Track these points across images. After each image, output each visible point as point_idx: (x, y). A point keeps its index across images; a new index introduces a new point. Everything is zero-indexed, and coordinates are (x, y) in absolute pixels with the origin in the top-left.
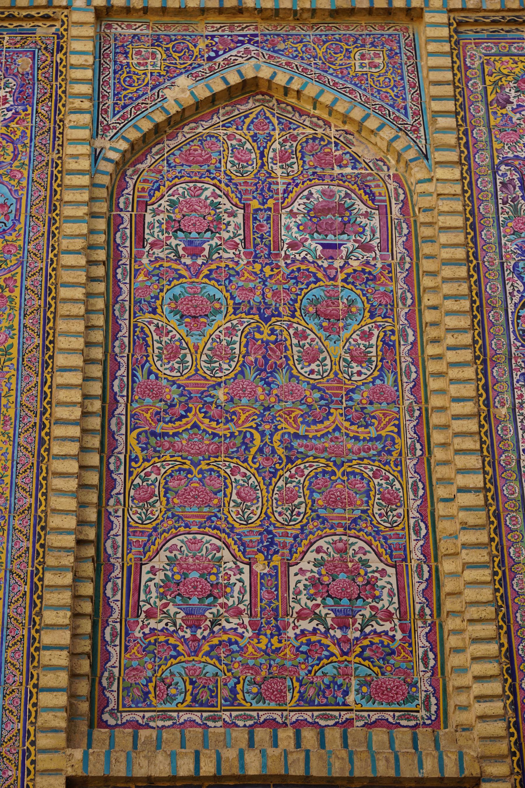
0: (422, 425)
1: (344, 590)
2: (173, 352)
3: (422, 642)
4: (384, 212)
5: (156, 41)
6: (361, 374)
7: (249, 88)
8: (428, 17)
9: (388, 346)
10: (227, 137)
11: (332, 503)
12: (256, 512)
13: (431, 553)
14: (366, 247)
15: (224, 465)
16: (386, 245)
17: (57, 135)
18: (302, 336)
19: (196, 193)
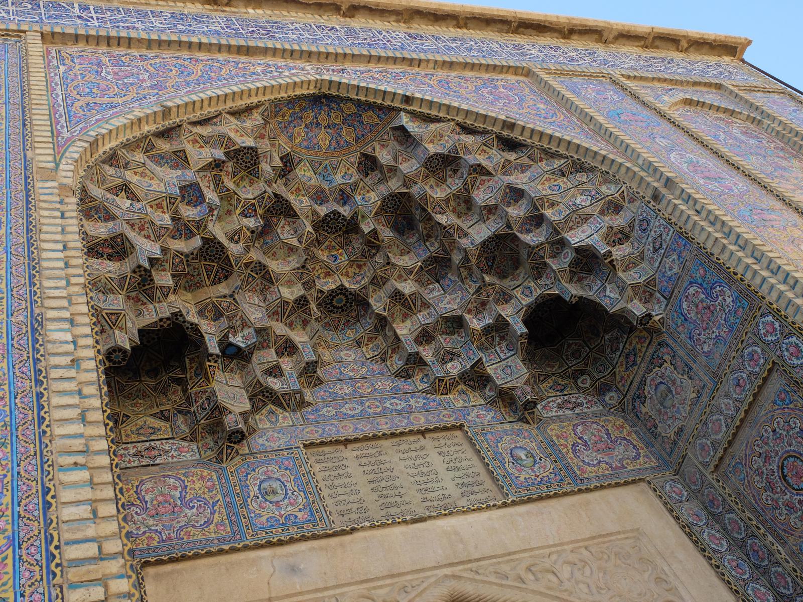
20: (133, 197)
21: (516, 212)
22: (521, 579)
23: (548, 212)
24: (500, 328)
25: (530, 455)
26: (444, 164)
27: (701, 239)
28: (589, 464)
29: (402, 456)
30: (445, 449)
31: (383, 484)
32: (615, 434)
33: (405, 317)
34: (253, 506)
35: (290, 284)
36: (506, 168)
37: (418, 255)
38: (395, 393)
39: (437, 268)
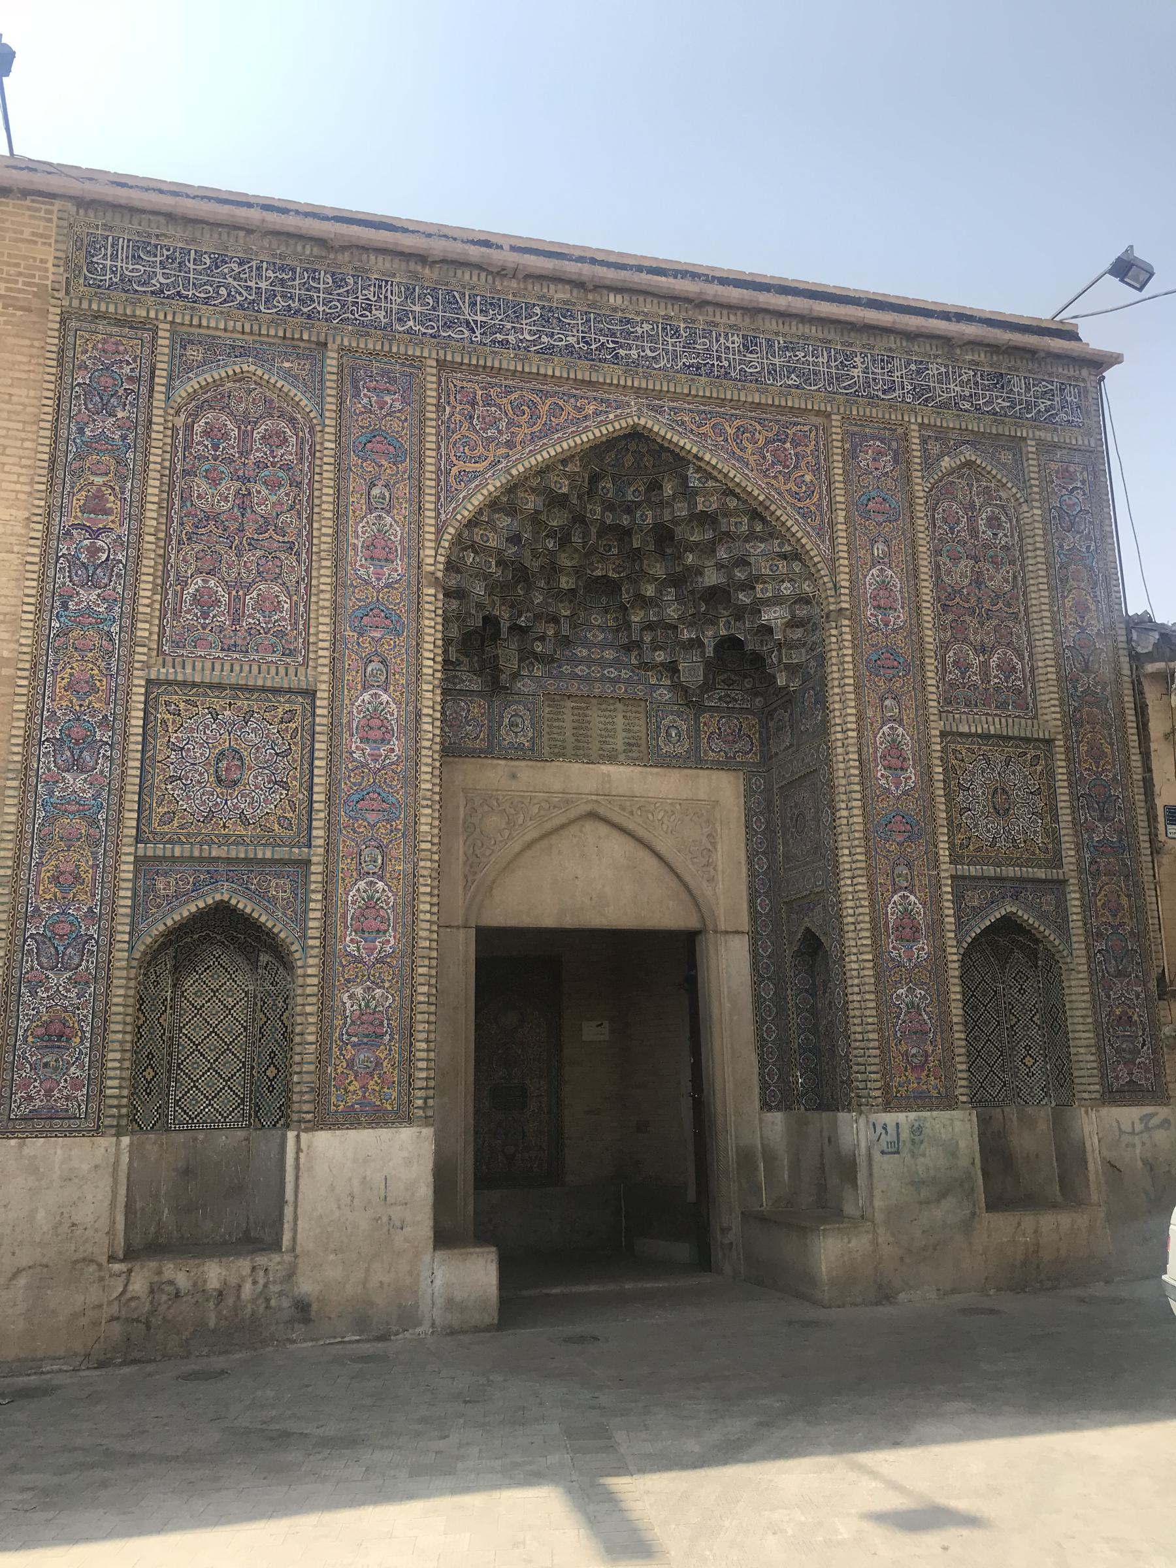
1: (1008, 670)
2: (949, 573)
3: (1029, 689)
5: (936, 439)
6: (1007, 587)
7: (969, 464)
9: (1015, 577)
11: (1002, 636)
12: (979, 638)
13: (1031, 656)
14: (1006, 536)
16: (1012, 536)
17: (909, 479)
18: (988, 570)
20: (476, 552)
21: (740, 575)
22: (632, 813)
23: (759, 587)
24: (697, 643)
25: (679, 734)
26: (706, 519)
27: (829, 670)
28: (713, 751)
29: (600, 713)
30: (629, 714)
31: (582, 732)
32: (745, 731)
33: (642, 608)
34: (503, 732)
35: (568, 575)
36: (751, 536)
37: (666, 567)
38: (615, 663)
39: (678, 580)
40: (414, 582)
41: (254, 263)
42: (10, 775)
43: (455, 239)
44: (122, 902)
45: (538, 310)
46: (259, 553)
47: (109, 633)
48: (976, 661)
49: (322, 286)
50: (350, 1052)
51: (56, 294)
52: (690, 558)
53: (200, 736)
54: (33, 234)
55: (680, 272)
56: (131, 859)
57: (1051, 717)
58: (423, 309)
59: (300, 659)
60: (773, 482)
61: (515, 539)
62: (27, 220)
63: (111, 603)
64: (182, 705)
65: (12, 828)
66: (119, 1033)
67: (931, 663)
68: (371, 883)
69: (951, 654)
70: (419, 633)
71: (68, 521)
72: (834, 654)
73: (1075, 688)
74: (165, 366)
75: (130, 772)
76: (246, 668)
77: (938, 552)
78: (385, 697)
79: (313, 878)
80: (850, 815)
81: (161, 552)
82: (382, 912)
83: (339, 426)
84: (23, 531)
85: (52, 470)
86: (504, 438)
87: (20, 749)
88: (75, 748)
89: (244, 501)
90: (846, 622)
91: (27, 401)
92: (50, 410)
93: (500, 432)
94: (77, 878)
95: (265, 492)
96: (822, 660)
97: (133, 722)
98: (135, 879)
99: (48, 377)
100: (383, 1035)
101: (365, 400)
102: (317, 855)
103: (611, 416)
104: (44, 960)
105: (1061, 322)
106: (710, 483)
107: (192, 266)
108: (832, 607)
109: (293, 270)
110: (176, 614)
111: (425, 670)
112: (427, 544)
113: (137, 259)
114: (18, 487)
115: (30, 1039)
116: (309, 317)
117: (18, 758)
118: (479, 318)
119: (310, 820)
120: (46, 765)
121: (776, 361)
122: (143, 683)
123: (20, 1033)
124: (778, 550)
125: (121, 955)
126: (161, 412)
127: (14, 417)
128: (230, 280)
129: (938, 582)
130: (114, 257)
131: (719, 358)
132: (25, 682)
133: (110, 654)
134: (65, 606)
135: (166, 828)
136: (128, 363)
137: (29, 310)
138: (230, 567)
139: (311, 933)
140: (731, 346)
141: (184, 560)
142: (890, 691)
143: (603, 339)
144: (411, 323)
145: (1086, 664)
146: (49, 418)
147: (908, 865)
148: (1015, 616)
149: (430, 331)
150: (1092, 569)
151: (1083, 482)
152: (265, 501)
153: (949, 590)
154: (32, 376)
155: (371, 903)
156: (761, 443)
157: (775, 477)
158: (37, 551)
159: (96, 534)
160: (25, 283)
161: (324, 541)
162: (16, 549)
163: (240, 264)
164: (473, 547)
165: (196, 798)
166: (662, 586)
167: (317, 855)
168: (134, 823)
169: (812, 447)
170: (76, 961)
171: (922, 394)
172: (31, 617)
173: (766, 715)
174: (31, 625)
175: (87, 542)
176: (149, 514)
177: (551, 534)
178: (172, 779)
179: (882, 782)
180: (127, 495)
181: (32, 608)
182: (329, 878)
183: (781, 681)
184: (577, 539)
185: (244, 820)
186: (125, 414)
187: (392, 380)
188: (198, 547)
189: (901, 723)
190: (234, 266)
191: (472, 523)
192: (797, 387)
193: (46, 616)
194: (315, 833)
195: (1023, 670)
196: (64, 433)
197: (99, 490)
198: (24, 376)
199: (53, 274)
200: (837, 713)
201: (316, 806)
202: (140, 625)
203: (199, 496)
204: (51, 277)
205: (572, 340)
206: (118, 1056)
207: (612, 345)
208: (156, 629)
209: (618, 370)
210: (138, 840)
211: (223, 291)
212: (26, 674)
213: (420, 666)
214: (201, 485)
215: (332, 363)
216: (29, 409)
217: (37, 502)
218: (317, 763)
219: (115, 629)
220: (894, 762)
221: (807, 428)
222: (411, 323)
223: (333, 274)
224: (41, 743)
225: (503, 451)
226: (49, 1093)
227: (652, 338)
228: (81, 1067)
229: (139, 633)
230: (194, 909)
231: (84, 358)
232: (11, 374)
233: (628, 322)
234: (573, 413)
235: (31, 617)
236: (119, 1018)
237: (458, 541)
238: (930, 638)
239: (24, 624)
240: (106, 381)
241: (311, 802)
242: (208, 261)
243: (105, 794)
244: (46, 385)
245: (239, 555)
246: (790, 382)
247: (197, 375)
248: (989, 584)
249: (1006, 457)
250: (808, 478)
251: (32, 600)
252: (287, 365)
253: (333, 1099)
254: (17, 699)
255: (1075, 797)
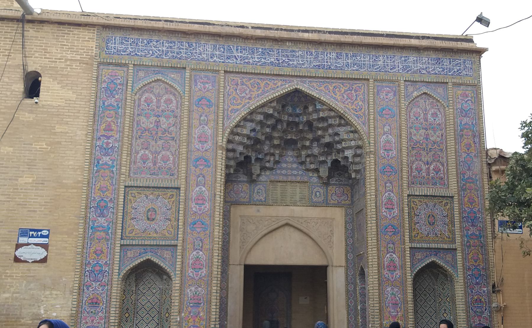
0: (446, 147)
1: (437, 170)
2: (415, 135)
4: (442, 114)
6: (439, 139)
8: (449, 84)
9: (442, 135)
10: (421, 101)
11: (436, 158)
12: (426, 159)
13: (447, 165)
15: (422, 152)
16: (442, 120)
19: (417, 110)
20: (239, 136)
24: (324, 162)
40: (215, 148)
41: (161, 41)
42: (81, 219)
43: (231, 26)
44: (116, 260)
45: (260, 50)
46: (163, 141)
47: (112, 171)
48: (424, 167)
49: (184, 48)
50: (190, 309)
51: (96, 58)
52: (320, 133)
53: (142, 203)
54: (89, 38)
55: (314, 31)
56: (119, 245)
57: (453, 189)
58: (220, 53)
59: (176, 177)
60: (347, 106)
61: (253, 130)
62: (87, 34)
63: (113, 160)
64: (136, 194)
65: (81, 236)
66: (115, 303)
67: (405, 169)
68: (198, 253)
69: (415, 165)
70: (216, 166)
71: (99, 134)
72: (368, 167)
73: (464, 177)
74: (131, 79)
75: (119, 217)
76: (157, 181)
77: (411, 128)
78: (204, 189)
79: (178, 251)
80: (371, 226)
81: (130, 142)
82: (201, 262)
83: (190, 97)
84: (85, 138)
85: (94, 117)
86: (248, 97)
87: (84, 210)
88: (101, 209)
89: (158, 123)
90: (373, 156)
91: (86, 94)
92: (93, 97)
93: (246, 94)
94: (102, 252)
95: (165, 120)
96: (365, 168)
97: (120, 200)
98: (120, 252)
99: (93, 86)
100: (200, 304)
101: (199, 87)
102: (180, 243)
103: (287, 86)
104: (91, 278)
105: (466, 35)
106: (324, 107)
107: (140, 44)
108: (368, 150)
109: (174, 42)
110: (135, 163)
111: (218, 179)
112: (220, 135)
113: (122, 43)
114: (84, 124)
115: (87, 304)
116: (180, 59)
117: (83, 213)
118: (240, 54)
119: (178, 231)
120: (92, 216)
121: (349, 61)
122: (123, 187)
123: (84, 302)
124: (349, 129)
125: (115, 277)
126: (130, 95)
127: (82, 100)
128: (153, 48)
129: (410, 139)
130: (115, 43)
131: (327, 62)
132: (86, 188)
133: (113, 177)
134: (98, 162)
135: (131, 235)
136: (119, 79)
137: (87, 64)
138: (153, 146)
139: (177, 269)
140: (332, 57)
141: (138, 145)
142: (389, 180)
143: (284, 59)
144: (215, 58)
145: (469, 167)
146: (93, 100)
147: (393, 244)
148: (442, 150)
149: (222, 61)
150: (473, 131)
151: (472, 97)
152: (164, 123)
153: (415, 141)
154: (88, 86)
155: (198, 259)
156: (343, 92)
157: (348, 104)
158: (89, 145)
159: (108, 138)
160: (86, 55)
161: (184, 137)
162: (83, 144)
163: (157, 42)
164: (238, 134)
165: (139, 225)
166: (312, 141)
167: (180, 243)
168: (120, 234)
169: (362, 92)
170: (101, 279)
171: (406, 69)
172: (87, 167)
173: (352, 187)
174: (87, 169)
175: (105, 141)
176: (126, 130)
177: (268, 126)
178: (133, 219)
179: (384, 213)
180: (119, 124)
181: (88, 164)
182: (184, 250)
183: (353, 176)
184: (279, 127)
185: (156, 232)
186: (118, 97)
187: (209, 79)
188: (142, 140)
189: (392, 192)
190: (155, 43)
191: (237, 126)
192: (357, 70)
193: (92, 166)
194: (179, 236)
195: (444, 170)
196: (98, 104)
197: (109, 123)
198: (86, 86)
199: (95, 51)
200: (369, 189)
201: (180, 226)
202: (123, 168)
203: (143, 123)
204: (94, 52)
205: (272, 60)
206: (114, 309)
207: (287, 61)
208: (128, 169)
209: (289, 69)
210: (122, 239)
211: (151, 52)
212: (86, 185)
213: (216, 178)
214: (143, 119)
215: (187, 74)
216: (87, 97)
217: (89, 128)
218: (180, 212)
219: (114, 169)
220: (390, 206)
221: (360, 85)
222: (215, 58)
223: (188, 43)
224: (91, 208)
225: (247, 101)
226: (93, 321)
227: (302, 57)
228: (103, 313)
229: (122, 171)
230: (139, 262)
231: (105, 78)
232: (82, 86)
233: (293, 51)
234: (273, 86)
235: (87, 167)
236: (115, 297)
237: (232, 133)
238: (405, 159)
239: (85, 169)
240: (112, 85)
241: (178, 225)
242: (146, 42)
243: (111, 224)
244: (93, 89)
245: (156, 142)
246: (354, 69)
247: (142, 82)
248: (431, 138)
249: (440, 90)
250: (360, 103)
251: (88, 161)
252: (173, 76)
253: (184, 325)
254: (83, 194)
255: (462, 219)
